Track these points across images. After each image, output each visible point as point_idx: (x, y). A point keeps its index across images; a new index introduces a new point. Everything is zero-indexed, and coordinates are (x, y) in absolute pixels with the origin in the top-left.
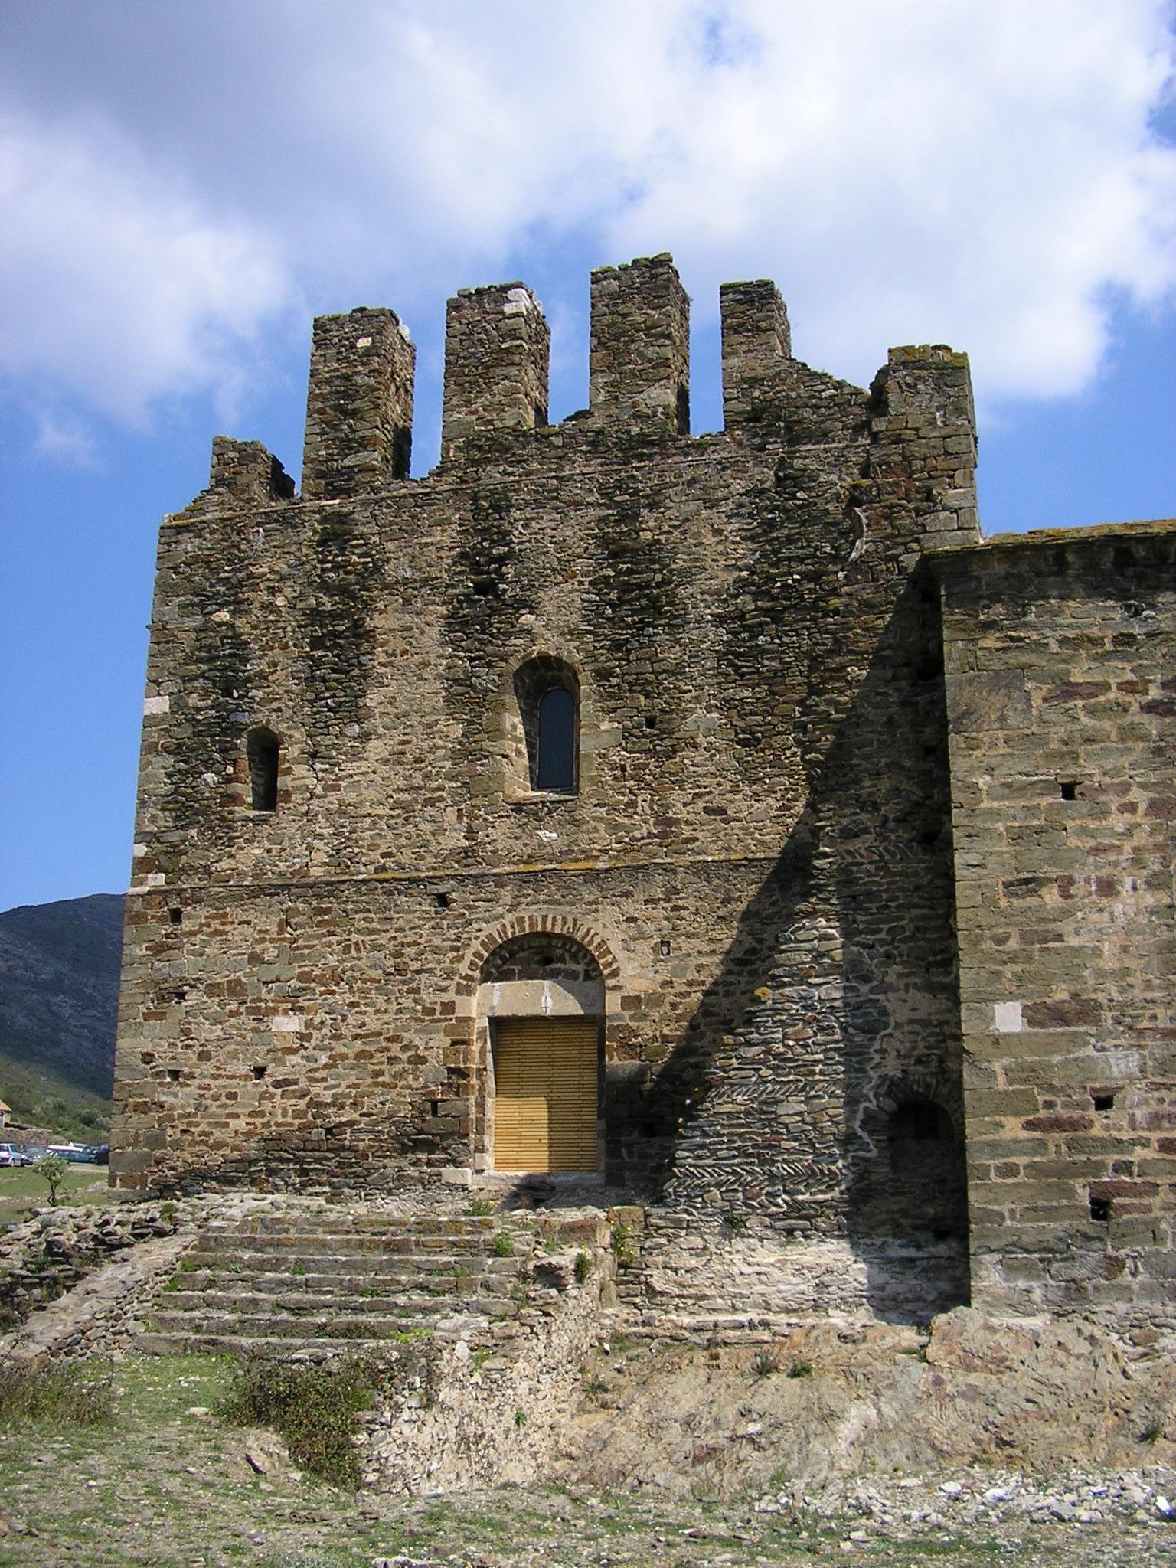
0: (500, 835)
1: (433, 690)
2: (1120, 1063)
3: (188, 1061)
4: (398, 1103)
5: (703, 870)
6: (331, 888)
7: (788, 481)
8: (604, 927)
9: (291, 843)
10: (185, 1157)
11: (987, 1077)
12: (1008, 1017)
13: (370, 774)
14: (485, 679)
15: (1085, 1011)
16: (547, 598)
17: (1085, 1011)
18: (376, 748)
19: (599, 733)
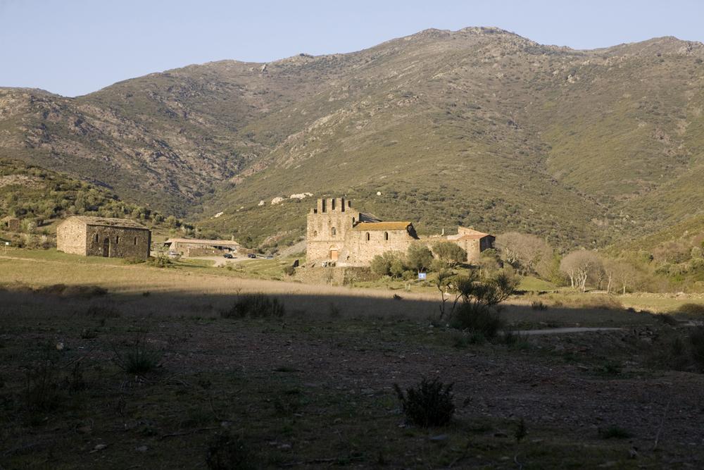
0: (331, 239)
9: (317, 238)
13: (323, 233)
19: (337, 232)
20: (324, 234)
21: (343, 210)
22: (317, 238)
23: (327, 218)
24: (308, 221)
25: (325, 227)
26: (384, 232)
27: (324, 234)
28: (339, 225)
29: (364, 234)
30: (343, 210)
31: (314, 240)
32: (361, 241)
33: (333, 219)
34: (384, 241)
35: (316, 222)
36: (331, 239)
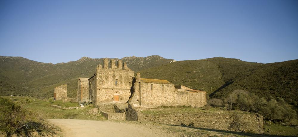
0: (115, 87)
1: (112, 80)
2: (145, 99)
3: (101, 96)
4: (111, 98)
5: (124, 89)
6: (107, 88)
7: (127, 73)
8: (120, 91)
10: (101, 101)
11: (141, 99)
12: (142, 98)
13: (109, 83)
14: (114, 80)
15: (144, 98)
16: (117, 76)
17: (144, 98)
18: (109, 82)
20: (110, 83)
21: (123, 69)
22: (105, 86)
23: (112, 73)
24: (97, 74)
25: (111, 79)
26: (162, 85)
27: (110, 83)
28: (121, 78)
29: (150, 85)
30: (123, 69)
31: (103, 87)
32: (148, 90)
33: (116, 73)
34: (162, 91)
35: (104, 74)
36: (115, 87)
